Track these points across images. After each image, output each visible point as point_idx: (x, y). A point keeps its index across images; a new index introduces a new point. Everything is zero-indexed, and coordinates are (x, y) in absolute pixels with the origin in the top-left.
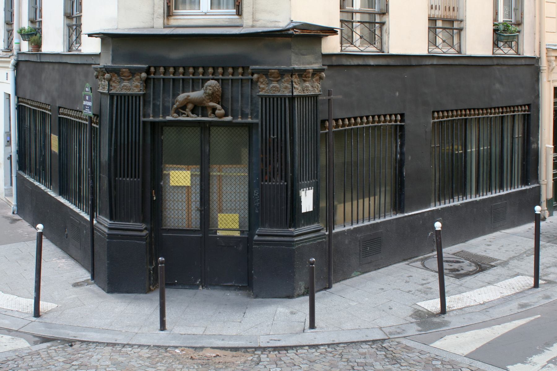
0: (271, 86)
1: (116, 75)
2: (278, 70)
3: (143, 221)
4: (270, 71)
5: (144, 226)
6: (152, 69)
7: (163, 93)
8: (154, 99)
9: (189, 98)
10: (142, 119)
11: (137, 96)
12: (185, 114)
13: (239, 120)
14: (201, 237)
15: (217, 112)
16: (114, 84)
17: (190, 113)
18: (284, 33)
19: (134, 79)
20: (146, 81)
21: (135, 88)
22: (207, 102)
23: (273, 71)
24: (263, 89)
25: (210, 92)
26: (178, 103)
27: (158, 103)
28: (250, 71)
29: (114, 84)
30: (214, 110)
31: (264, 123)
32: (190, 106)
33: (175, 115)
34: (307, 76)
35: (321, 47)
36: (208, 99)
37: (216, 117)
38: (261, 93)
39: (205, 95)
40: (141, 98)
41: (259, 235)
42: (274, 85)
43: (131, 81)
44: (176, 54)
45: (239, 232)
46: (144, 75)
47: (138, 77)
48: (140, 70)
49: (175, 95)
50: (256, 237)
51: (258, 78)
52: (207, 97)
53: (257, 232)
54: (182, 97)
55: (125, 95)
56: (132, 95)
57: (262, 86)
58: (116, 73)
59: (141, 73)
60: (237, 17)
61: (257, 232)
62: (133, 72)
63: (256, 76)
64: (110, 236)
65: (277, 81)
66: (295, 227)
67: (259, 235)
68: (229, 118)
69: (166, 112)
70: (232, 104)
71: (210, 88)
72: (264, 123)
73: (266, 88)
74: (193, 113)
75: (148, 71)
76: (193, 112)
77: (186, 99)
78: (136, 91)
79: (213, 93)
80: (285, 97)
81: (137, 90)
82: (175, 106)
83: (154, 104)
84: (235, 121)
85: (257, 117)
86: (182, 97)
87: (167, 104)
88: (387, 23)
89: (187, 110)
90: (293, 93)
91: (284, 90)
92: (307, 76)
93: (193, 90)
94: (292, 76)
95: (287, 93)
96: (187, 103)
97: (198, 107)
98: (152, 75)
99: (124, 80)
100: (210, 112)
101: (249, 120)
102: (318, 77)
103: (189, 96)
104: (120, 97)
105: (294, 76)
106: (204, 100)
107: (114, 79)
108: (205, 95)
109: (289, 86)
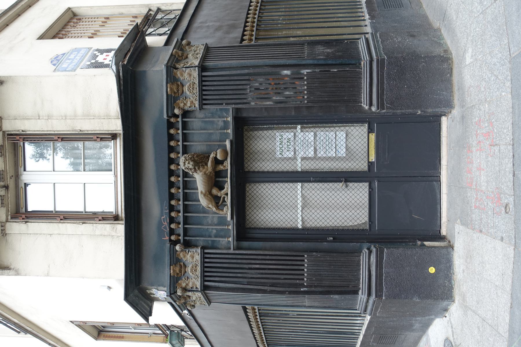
0: (188, 93)
1: (179, 282)
2: (167, 83)
3: (359, 251)
4: (169, 92)
5: (365, 251)
6: (173, 238)
7: (202, 225)
8: (210, 237)
9: (204, 191)
10: (232, 251)
11: (204, 256)
12: (224, 198)
13: (230, 131)
14: (379, 181)
15: (219, 157)
16: (190, 285)
17: (223, 192)
18: (122, 78)
19: (184, 260)
20: (188, 245)
21: (195, 260)
22: (207, 169)
23: (169, 90)
24: (192, 102)
25: (192, 163)
26: (210, 206)
27: (215, 231)
28: (172, 120)
29: (190, 285)
30: (217, 162)
31: (233, 101)
32: (215, 191)
33: (225, 209)
34: (180, 55)
35: (159, 47)
36: (204, 168)
37: (226, 159)
38: (197, 105)
39: (198, 172)
40: (206, 251)
41: (371, 104)
42: (186, 89)
43: (186, 263)
44: (154, 207)
45: (370, 134)
46: (178, 248)
47: (181, 255)
48: (173, 253)
49: (204, 211)
50: (374, 109)
51: (179, 108)
52: (201, 169)
53: (367, 108)
54: (204, 202)
55: (203, 272)
56: (203, 263)
57: (189, 104)
58: (177, 282)
59: (177, 251)
60: (118, 140)
61: (367, 108)
62: (175, 260)
63: (176, 111)
64: (379, 295)
65: (183, 86)
66: (360, 59)
67: (371, 104)
68: (228, 144)
69: (222, 221)
70: (213, 142)
71: (186, 164)
72: (233, 101)
73: (191, 98)
74: (223, 188)
75: (174, 243)
76: (221, 188)
77: (205, 195)
78: (198, 257)
79: (194, 161)
80: (201, 77)
81: (197, 256)
82: (214, 209)
83: (216, 237)
84: (231, 137)
85: (227, 110)
86: (204, 202)
87: (216, 221)
88: (158, 6)
89: (219, 195)
90: (196, 67)
91: (192, 77)
92: (180, 55)
93: (197, 189)
94: (177, 69)
95: (195, 74)
96: (210, 193)
97: (215, 181)
98: (180, 238)
99: (185, 272)
100: (221, 167)
101: (230, 119)
102: (187, 47)
103: (202, 192)
104: (204, 277)
105: (177, 66)
106: (205, 173)
107: (184, 285)
108: (198, 172)
109: (188, 70)
